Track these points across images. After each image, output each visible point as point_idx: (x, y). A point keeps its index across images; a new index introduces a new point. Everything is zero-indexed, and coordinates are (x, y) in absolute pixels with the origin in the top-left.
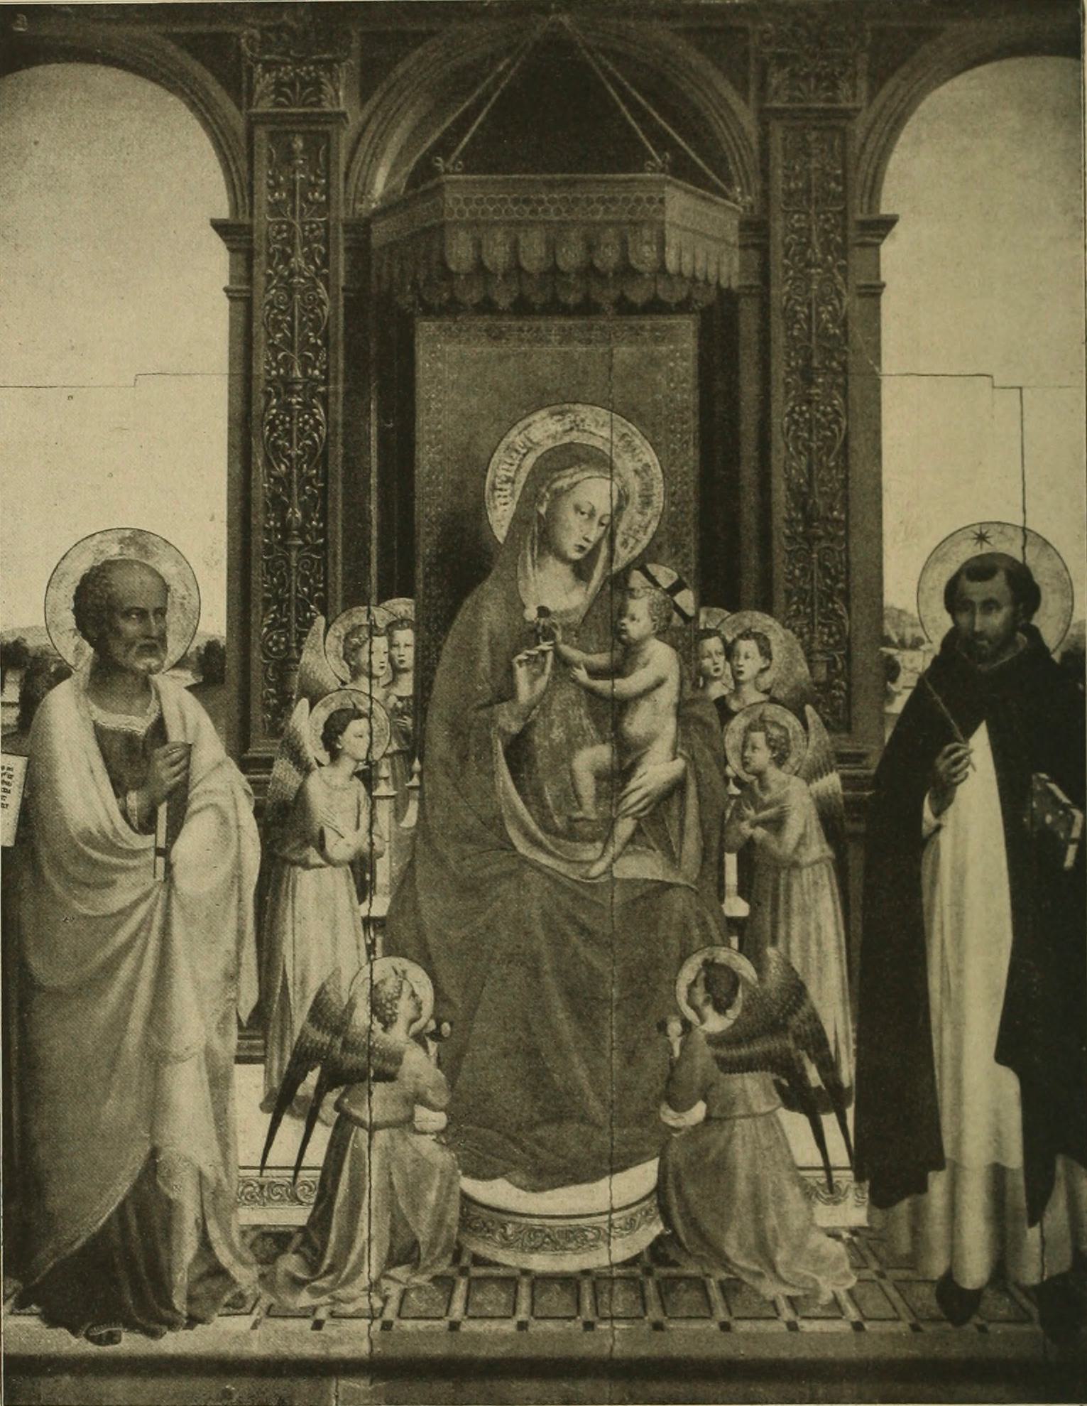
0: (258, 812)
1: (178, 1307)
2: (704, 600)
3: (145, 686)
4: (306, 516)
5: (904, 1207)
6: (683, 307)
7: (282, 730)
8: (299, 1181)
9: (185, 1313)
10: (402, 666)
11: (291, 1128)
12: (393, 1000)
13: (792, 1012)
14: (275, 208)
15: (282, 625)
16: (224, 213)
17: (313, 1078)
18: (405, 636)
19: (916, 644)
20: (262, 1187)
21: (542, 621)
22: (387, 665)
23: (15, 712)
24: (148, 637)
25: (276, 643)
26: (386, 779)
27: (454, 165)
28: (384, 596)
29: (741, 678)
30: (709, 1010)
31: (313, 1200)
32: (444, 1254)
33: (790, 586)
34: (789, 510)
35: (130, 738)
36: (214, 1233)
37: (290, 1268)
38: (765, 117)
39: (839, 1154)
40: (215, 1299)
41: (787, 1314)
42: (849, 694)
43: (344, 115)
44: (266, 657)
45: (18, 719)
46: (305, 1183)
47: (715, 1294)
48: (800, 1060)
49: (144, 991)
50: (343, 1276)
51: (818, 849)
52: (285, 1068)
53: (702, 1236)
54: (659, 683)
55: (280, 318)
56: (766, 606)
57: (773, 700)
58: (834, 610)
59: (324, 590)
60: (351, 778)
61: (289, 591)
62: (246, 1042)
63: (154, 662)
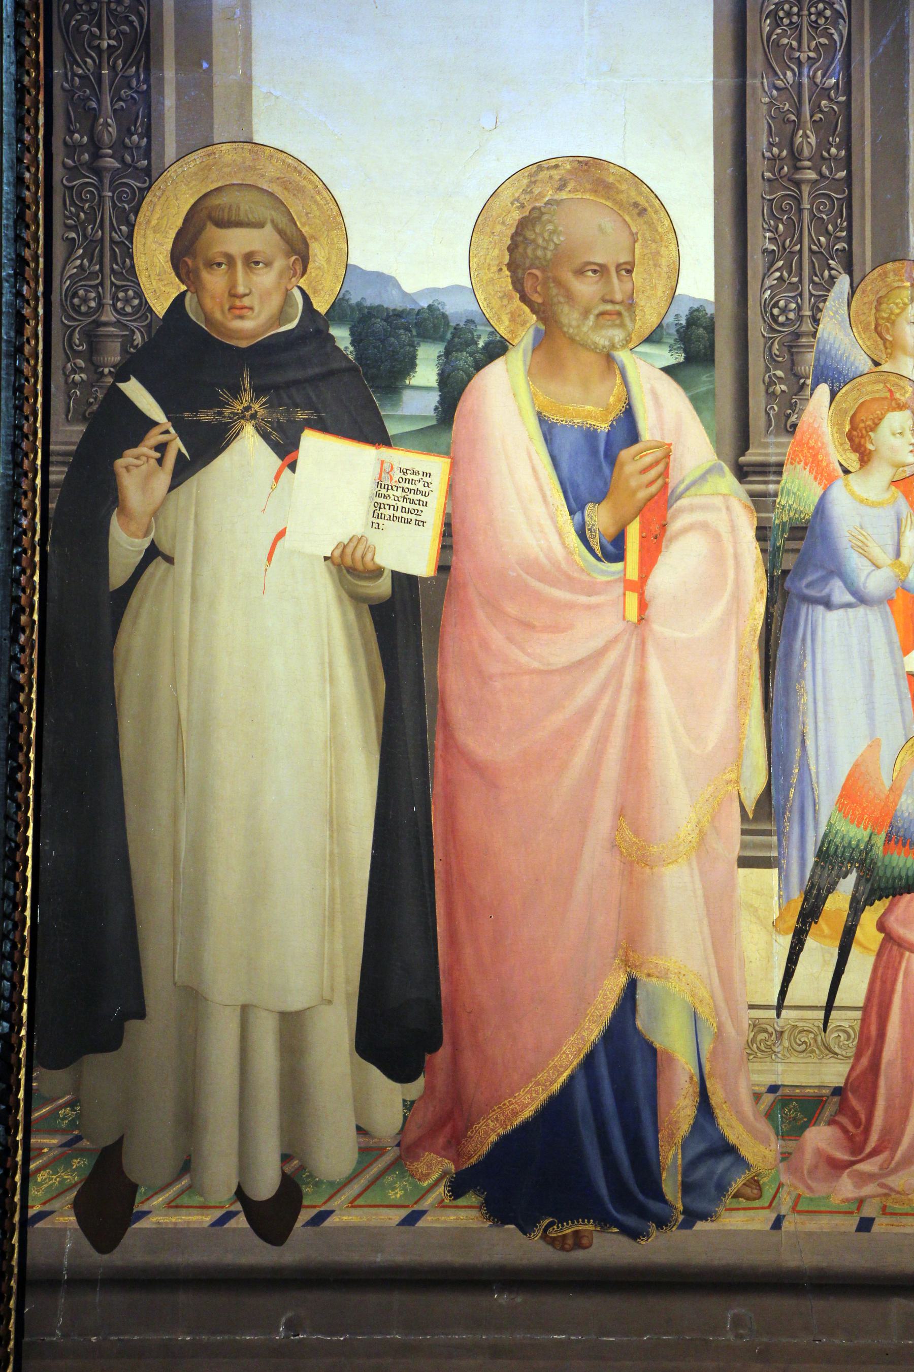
0: (762, 533)
1: (669, 1197)
4: (824, 144)
7: (794, 426)
8: (831, 1025)
9: (680, 1207)
15: (793, 286)
17: (847, 886)
23: (434, 398)
24: (612, 302)
25: (784, 311)
31: (851, 1052)
35: (591, 435)
36: (717, 1097)
37: (823, 1145)
40: (722, 1188)
45: (436, 409)
49: (611, 770)
52: (808, 876)
59: (849, 240)
61: (800, 242)
63: (618, 335)
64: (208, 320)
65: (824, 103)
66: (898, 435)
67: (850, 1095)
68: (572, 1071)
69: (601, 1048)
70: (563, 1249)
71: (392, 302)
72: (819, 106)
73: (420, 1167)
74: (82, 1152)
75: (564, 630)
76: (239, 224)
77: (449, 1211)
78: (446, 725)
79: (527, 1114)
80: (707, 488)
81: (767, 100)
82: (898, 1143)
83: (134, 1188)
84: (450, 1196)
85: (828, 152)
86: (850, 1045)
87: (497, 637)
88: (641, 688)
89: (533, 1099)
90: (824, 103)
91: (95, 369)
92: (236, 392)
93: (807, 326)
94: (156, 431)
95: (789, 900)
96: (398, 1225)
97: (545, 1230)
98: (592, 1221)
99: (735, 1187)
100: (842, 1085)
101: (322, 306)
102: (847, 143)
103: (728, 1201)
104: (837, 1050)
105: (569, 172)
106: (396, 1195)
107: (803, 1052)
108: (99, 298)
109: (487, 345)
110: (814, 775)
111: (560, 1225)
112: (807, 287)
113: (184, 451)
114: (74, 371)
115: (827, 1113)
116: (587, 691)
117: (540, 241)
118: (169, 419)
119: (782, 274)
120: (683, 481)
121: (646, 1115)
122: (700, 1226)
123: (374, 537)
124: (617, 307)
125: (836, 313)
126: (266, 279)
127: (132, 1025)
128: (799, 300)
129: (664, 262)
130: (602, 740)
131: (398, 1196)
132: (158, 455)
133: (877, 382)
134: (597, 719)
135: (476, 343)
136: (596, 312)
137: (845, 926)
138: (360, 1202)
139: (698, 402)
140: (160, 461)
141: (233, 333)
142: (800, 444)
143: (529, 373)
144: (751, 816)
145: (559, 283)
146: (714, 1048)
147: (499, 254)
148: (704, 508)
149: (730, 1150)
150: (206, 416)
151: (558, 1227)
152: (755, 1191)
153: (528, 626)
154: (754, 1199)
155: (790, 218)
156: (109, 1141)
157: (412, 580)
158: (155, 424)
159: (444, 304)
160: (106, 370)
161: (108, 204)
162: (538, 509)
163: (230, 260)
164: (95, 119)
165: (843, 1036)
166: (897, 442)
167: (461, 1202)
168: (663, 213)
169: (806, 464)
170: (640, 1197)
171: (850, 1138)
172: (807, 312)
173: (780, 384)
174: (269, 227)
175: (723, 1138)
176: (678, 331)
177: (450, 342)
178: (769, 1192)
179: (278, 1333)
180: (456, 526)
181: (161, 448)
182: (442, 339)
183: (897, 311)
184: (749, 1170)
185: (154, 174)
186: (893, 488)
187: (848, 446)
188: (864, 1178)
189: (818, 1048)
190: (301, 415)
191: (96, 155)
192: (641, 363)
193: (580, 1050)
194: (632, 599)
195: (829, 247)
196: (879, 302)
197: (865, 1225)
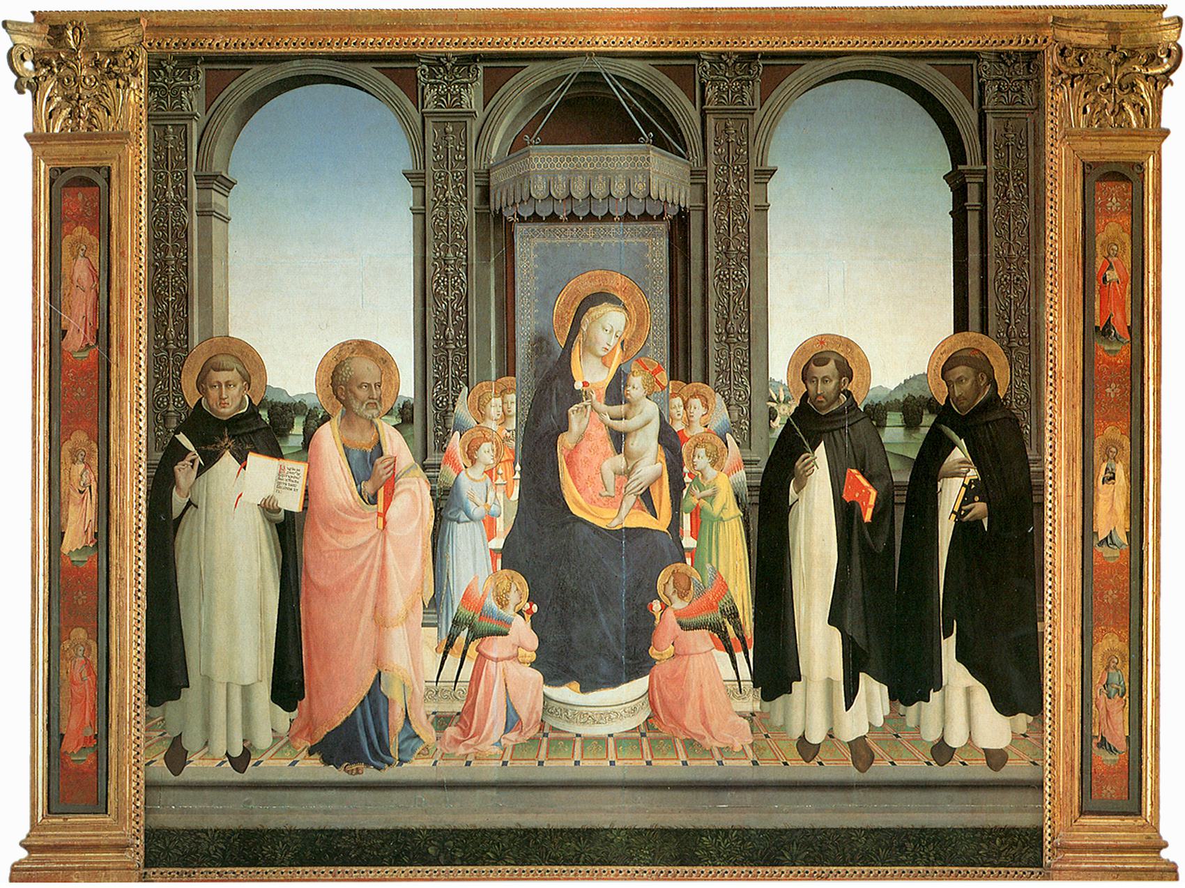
0: (432, 492)
1: (393, 754)
2: (672, 377)
4: (457, 334)
5: (779, 701)
6: (661, 217)
7: (445, 449)
10: (510, 414)
11: (453, 661)
13: (719, 598)
14: (437, 163)
16: (410, 167)
17: (464, 634)
18: (512, 397)
19: (785, 402)
20: (437, 692)
21: (585, 388)
22: (501, 413)
24: (373, 399)
27: (535, 139)
29: (692, 419)
30: (675, 597)
32: (535, 726)
33: (718, 369)
34: (718, 328)
38: (703, 114)
39: (745, 673)
40: (413, 751)
41: (718, 757)
42: (750, 429)
43: (475, 112)
44: (437, 410)
47: (679, 746)
48: (723, 622)
51: (734, 511)
53: (671, 716)
54: (647, 423)
55: (441, 224)
56: (705, 380)
57: (709, 431)
58: (742, 382)
61: (448, 373)
63: (375, 412)
69: (367, 698)
71: (284, 400)
74: (165, 738)
75: (353, 533)
76: (223, 370)
78: (306, 572)
79: (339, 723)
82: (482, 733)
87: (326, 536)
88: (384, 556)
92: (222, 438)
93: (451, 408)
94: (190, 454)
99: (418, 752)
101: (256, 402)
103: (416, 755)
108: (168, 401)
112: (451, 391)
115: (454, 723)
116: (363, 557)
121: (384, 723)
122: (404, 764)
123: (277, 496)
126: (234, 391)
130: (369, 577)
140: (192, 467)
141: (222, 414)
142: (447, 456)
145: (351, 391)
147: (327, 378)
149: (418, 736)
153: (339, 531)
157: (292, 513)
158: (190, 451)
161: (171, 362)
164: (166, 329)
167: (312, 757)
170: (382, 754)
172: (451, 402)
177: (307, 416)
181: (193, 461)
182: (304, 414)
185: (190, 350)
188: (468, 747)
191: (166, 344)
192: (384, 423)
195: (460, 376)
196: (479, 398)
197: (468, 764)
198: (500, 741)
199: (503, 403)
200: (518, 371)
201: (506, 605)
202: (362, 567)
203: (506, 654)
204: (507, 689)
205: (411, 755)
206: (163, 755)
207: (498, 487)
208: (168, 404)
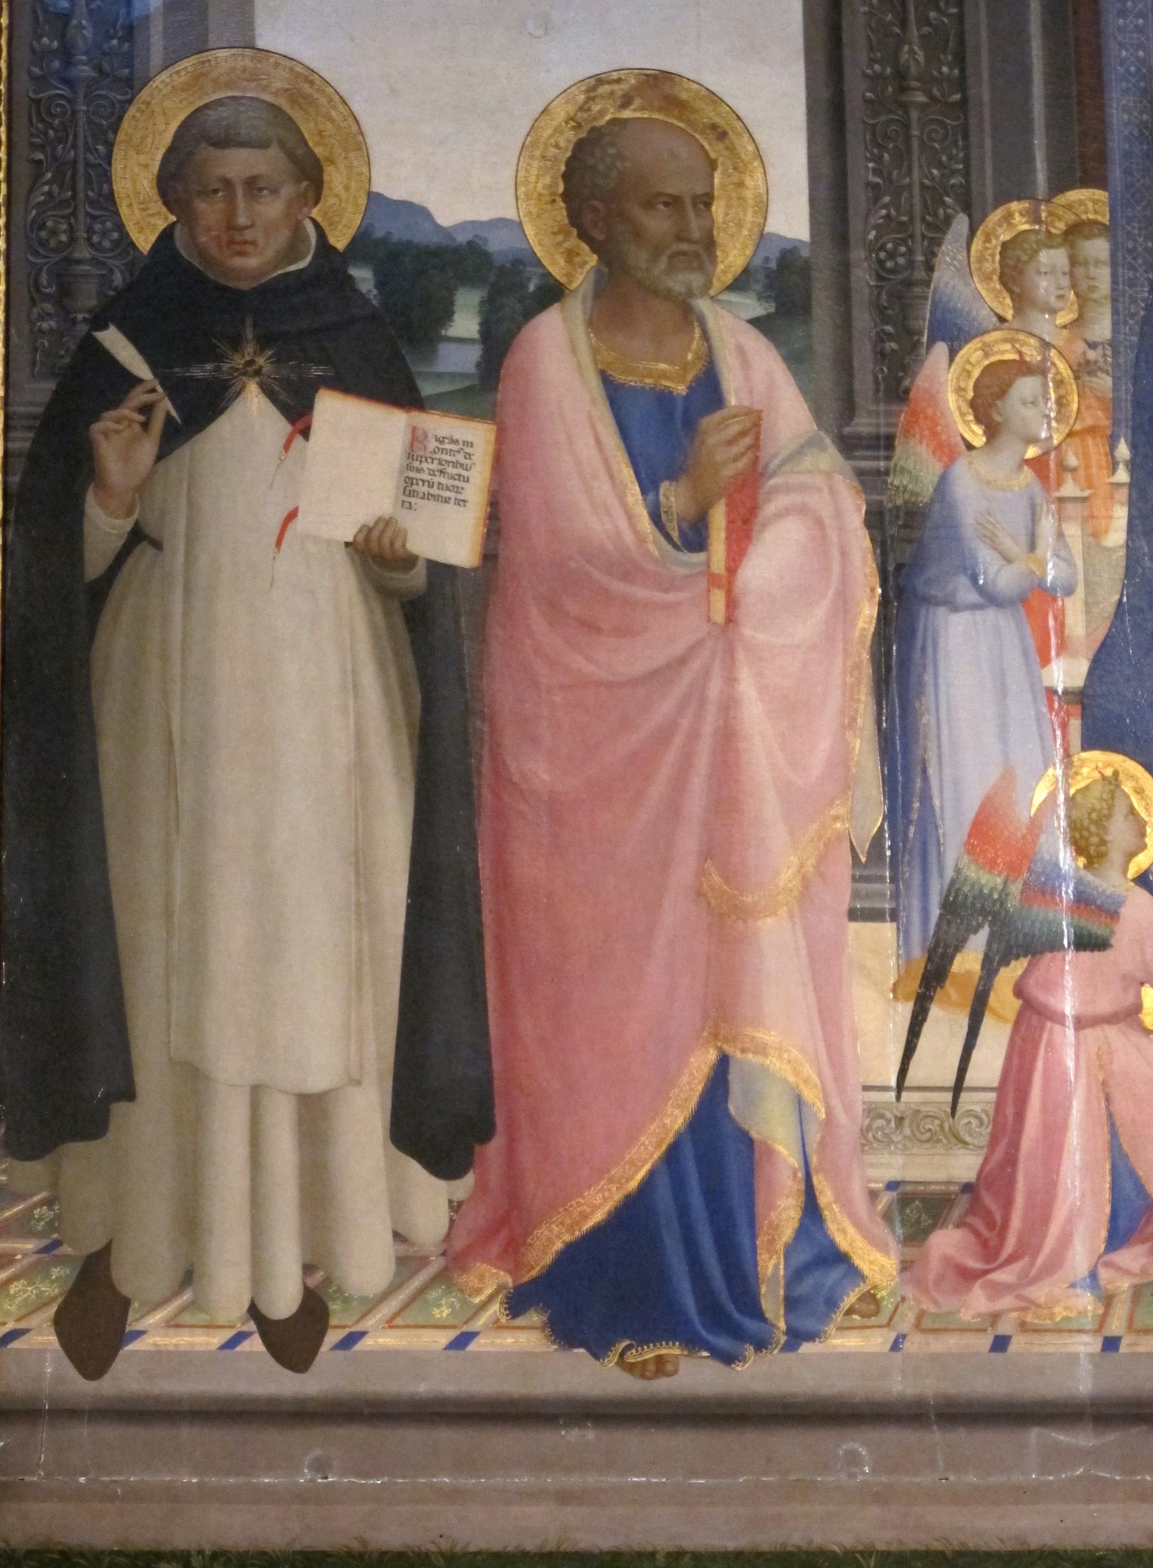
1: (769, 1315)
3: (687, 315)
7: (907, 391)
8: (960, 1110)
12: (1102, 820)
18: (1098, 248)
20: (900, 1120)
24: (689, 241)
25: (892, 255)
26: (1074, 470)
28: (1060, 183)
31: (984, 1141)
35: (664, 398)
36: (825, 1196)
37: (951, 1251)
40: (832, 1303)
45: (478, 365)
46: (969, 1113)
49: (695, 803)
50: (1040, 1260)
59: (967, 173)
60: (1020, 467)
62: (863, 887)
63: (696, 280)
64: (202, 253)
65: (932, 14)
66: (1030, 405)
67: (983, 1192)
68: (653, 1166)
70: (643, 1376)
71: (423, 237)
72: (927, 18)
73: (469, 1280)
74: (63, 1260)
76: (243, 144)
77: (506, 1333)
79: (598, 1217)
80: (807, 462)
81: (866, 9)
83: (126, 1303)
84: (507, 1315)
85: (940, 73)
86: (983, 1133)
89: (605, 1199)
90: (932, 14)
91: (66, 314)
92: (236, 343)
93: (920, 274)
94: (139, 389)
95: (909, 961)
96: (446, 1349)
97: (622, 1355)
98: (677, 1343)
100: (973, 1180)
101: (340, 241)
102: (960, 60)
103: (838, 1317)
104: (968, 1139)
105: (635, 88)
106: (443, 1313)
107: (928, 1141)
108: (71, 230)
109: (539, 288)
110: (937, 810)
111: (639, 1349)
112: (919, 228)
113: (174, 413)
114: (41, 318)
115: (957, 1213)
117: (601, 168)
118: (155, 375)
119: (889, 211)
120: (774, 456)
121: (741, 1219)
122: (806, 1348)
124: (693, 248)
125: (953, 259)
126: (272, 209)
127: (119, 1109)
128: (910, 243)
129: (749, 194)
131: (444, 1315)
132: (141, 418)
133: (1005, 341)
134: (678, 740)
135: (524, 286)
136: (669, 252)
137: (976, 991)
138: (399, 1321)
139: (796, 360)
140: (145, 426)
143: (590, 323)
144: (863, 859)
146: (823, 1138)
148: (803, 488)
150: (199, 372)
151: (637, 1351)
152: (872, 1307)
153: (592, 627)
154: (869, 1316)
155: (897, 147)
156: (94, 1246)
158: (139, 381)
159: (486, 240)
160: (80, 316)
162: (603, 487)
163: (228, 183)
165: (974, 1122)
166: (1029, 413)
167: (520, 1321)
168: (746, 137)
169: (922, 436)
170: (736, 1315)
171: (984, 1244)
172: (920, 258)
173: (889, 341)
174: (274, 151)
175: (833, 1245)
176: (767, 277)
178: (888, 1305)
179: (303, 1475)
180: (504, 506)
181: (146, 410)
183: (1025, 258)
184: (864, 1282)
185: (137, 84)
186: (1026, 468)
187: (971, 417)
188: (998, 1290)
189: (946, 1138)
190: (316, 372)
193: (662, 1140)
194: (718, 599)
197: (1000, 1344)
198: (1093, 1275)
199: (1074, 261)
200: (1116, 173)
201: (1102, 856)
202: (664, 735)
203: (1105, 1005)
204: (1110, 1115)
205: (825, 1318)
206: (54, 1308)
207: (1070, 508)
208: (72, 239)
